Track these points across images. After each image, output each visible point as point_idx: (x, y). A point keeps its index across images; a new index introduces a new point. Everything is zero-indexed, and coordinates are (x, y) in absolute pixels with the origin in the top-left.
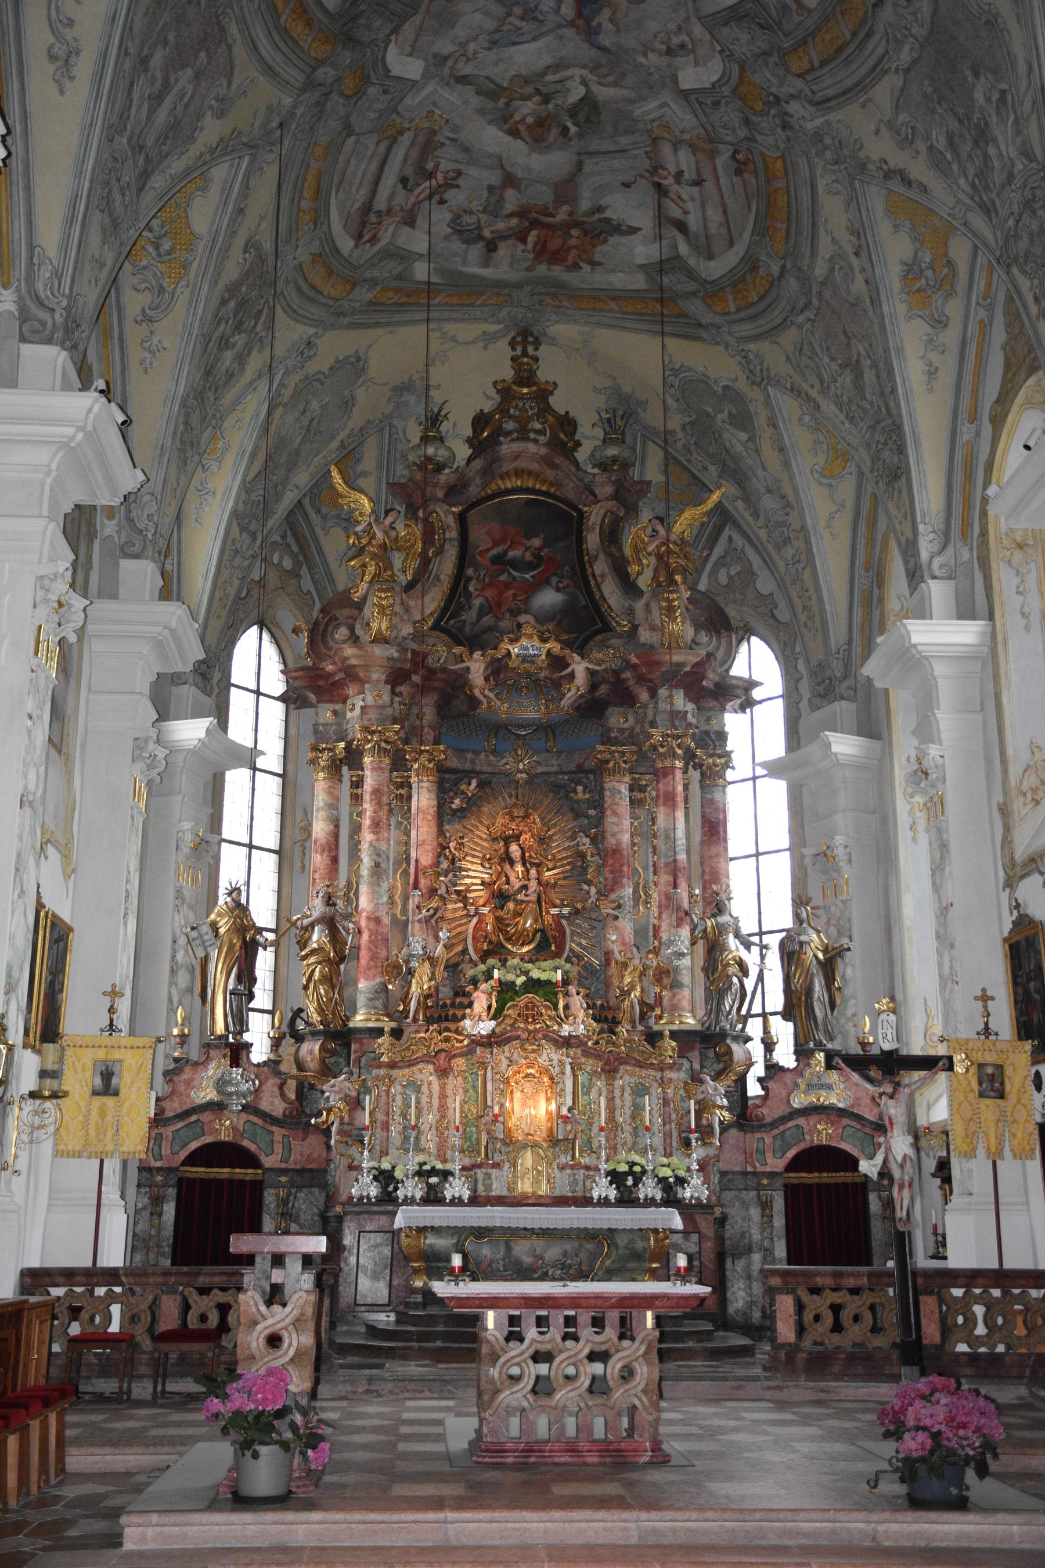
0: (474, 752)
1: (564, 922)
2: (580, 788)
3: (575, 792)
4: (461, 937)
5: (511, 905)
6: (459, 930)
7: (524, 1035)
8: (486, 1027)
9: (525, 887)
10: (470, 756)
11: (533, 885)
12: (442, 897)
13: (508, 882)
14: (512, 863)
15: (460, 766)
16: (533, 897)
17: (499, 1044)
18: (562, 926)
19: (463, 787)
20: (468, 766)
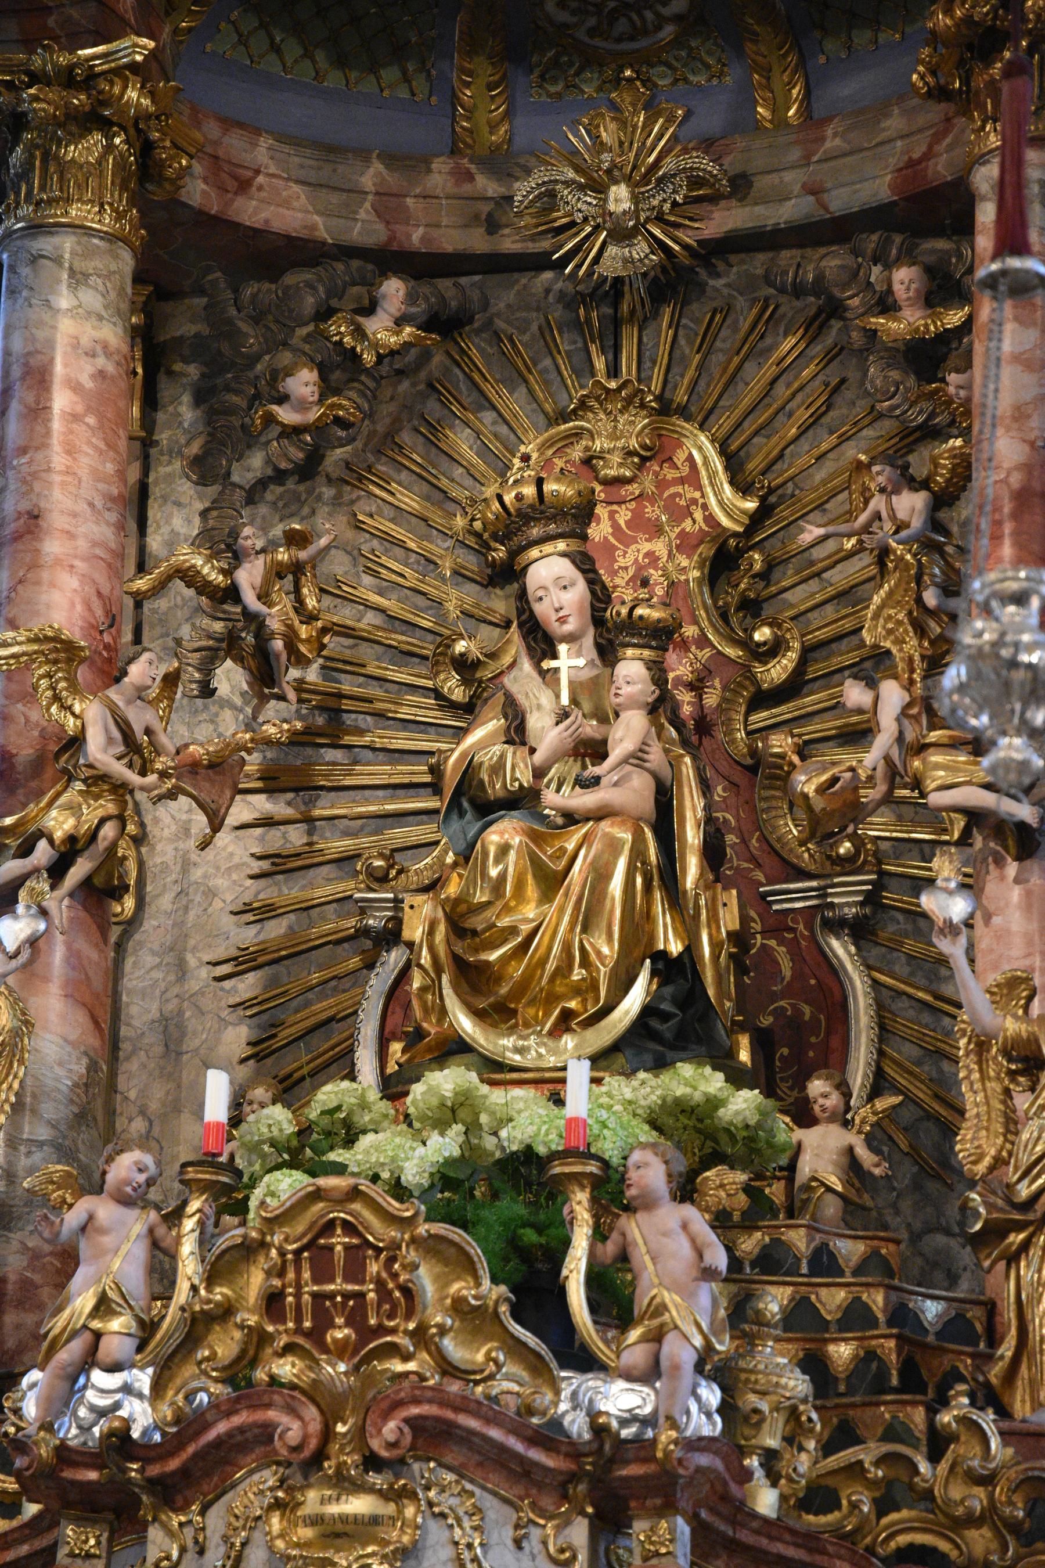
0: (390, 159)
1: (840, 948)
2: (904, 279)
3: (887, 305)
4: (322, 1044)
5: (506, 832)
6: (323, 1007)
7: (294, 1429)
8: (125, 1398)
9: (594, 750)
10: (371, 176)
11: (629, 731)
12: (99, 782)
13: (517, 733)
14: (541, 643)
15: (323, 229)
16: (635, 792)
17: (170, 1493)
18: (833, 970)
19: (339, 329)
20: (364, 228)
